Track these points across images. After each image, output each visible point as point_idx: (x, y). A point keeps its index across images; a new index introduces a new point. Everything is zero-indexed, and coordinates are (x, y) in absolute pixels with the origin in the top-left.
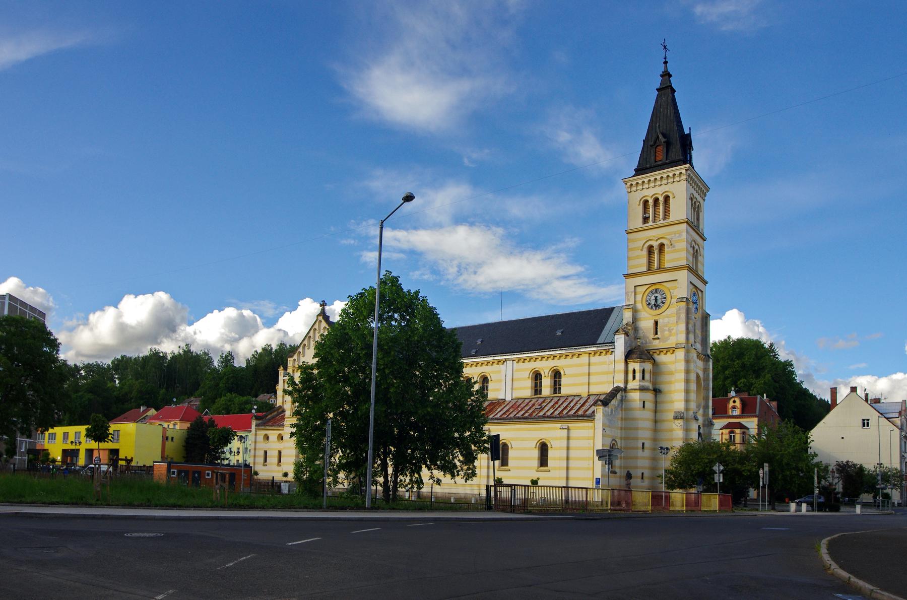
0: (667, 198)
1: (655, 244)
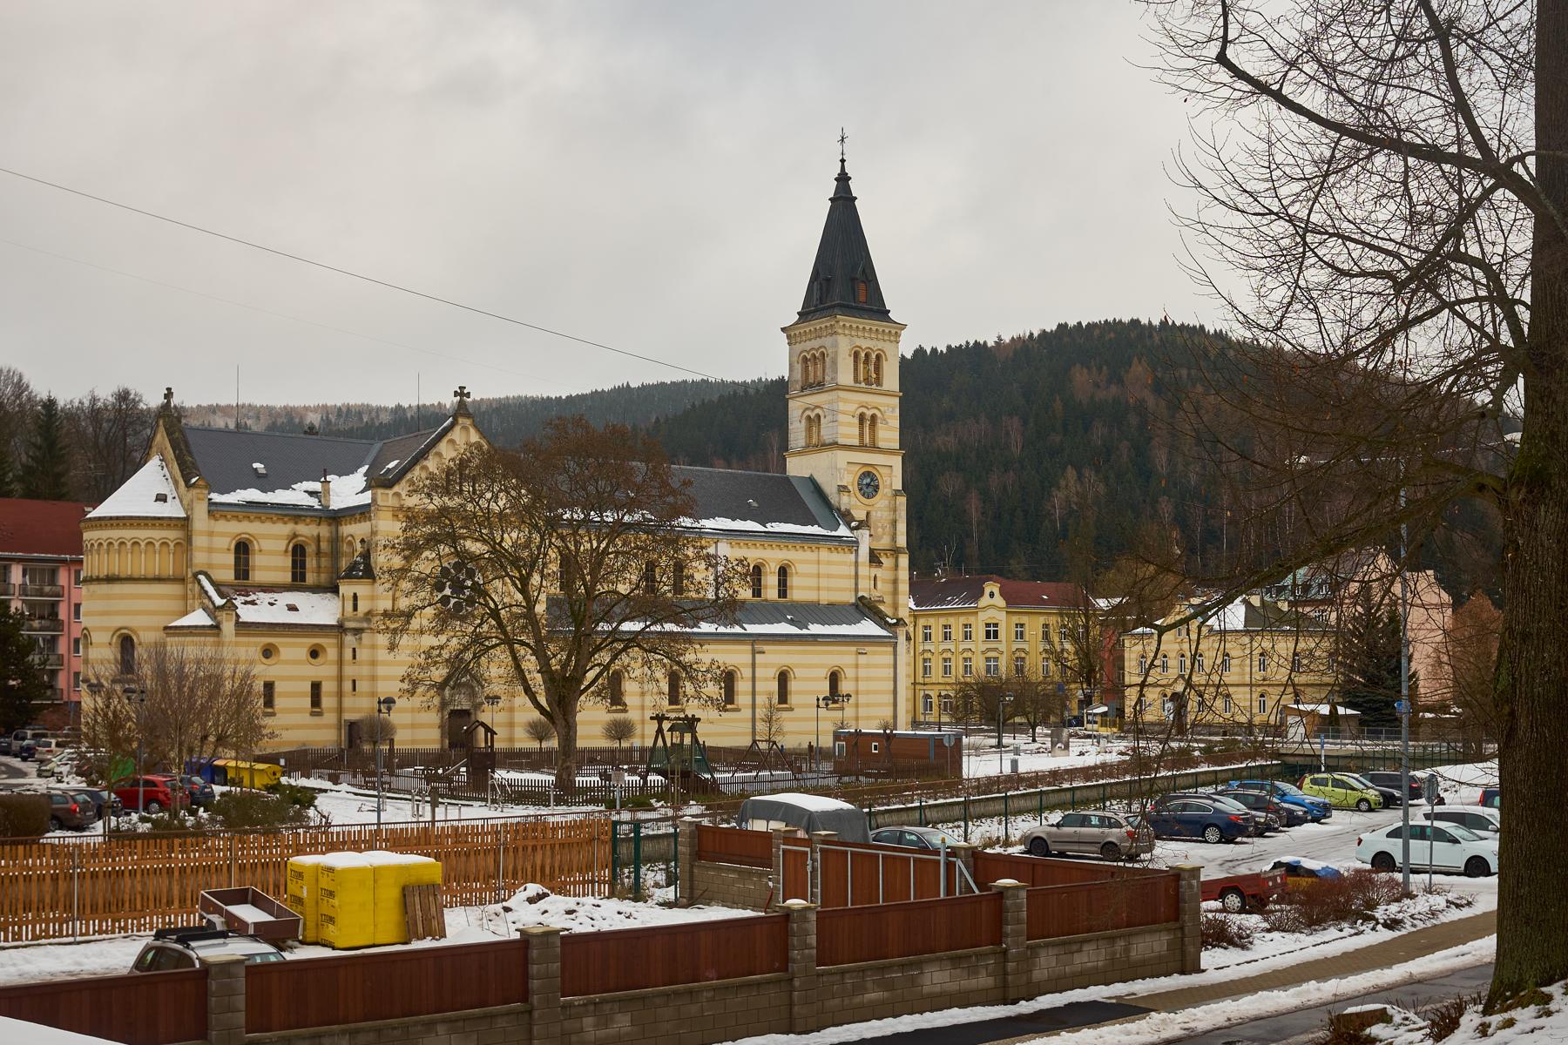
0: (878, 357)
1: (869, 413)
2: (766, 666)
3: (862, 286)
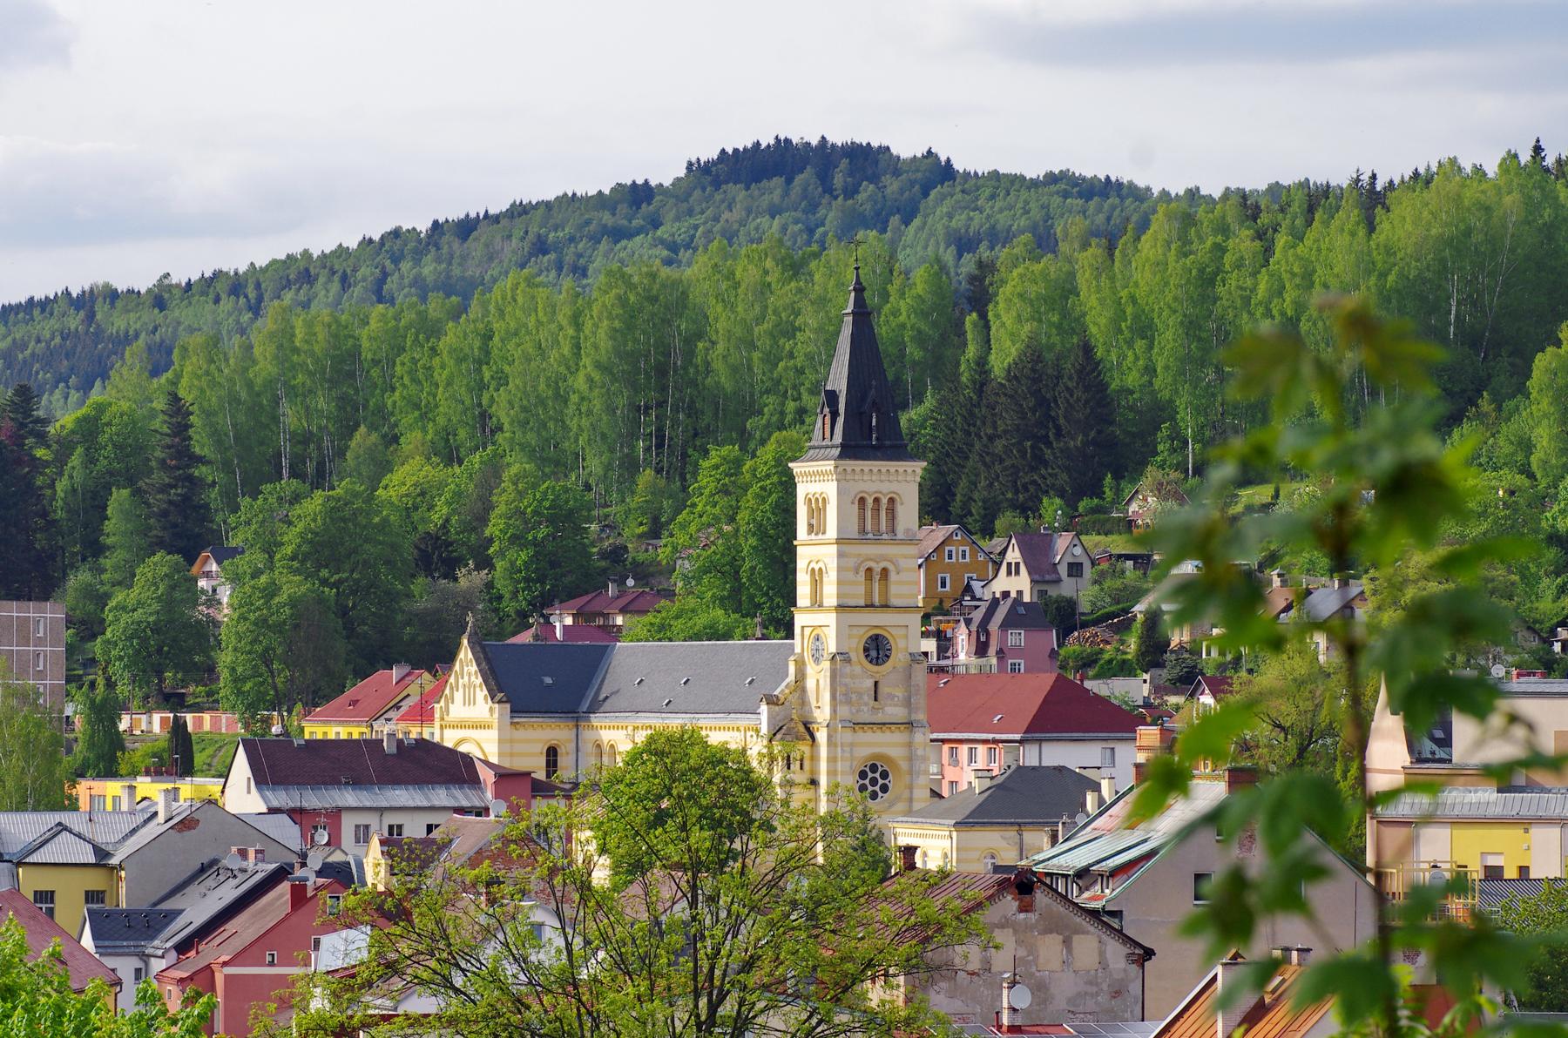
0: (891, 500)
1: (877, 568)
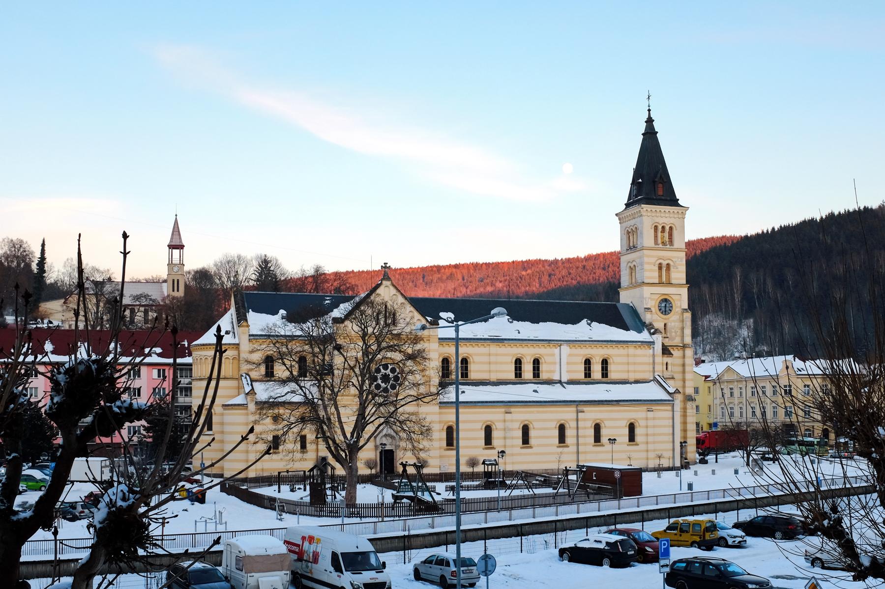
0: (671, 228)
1: (664, 263)
2: (585, 420)
3: (660, 185)
